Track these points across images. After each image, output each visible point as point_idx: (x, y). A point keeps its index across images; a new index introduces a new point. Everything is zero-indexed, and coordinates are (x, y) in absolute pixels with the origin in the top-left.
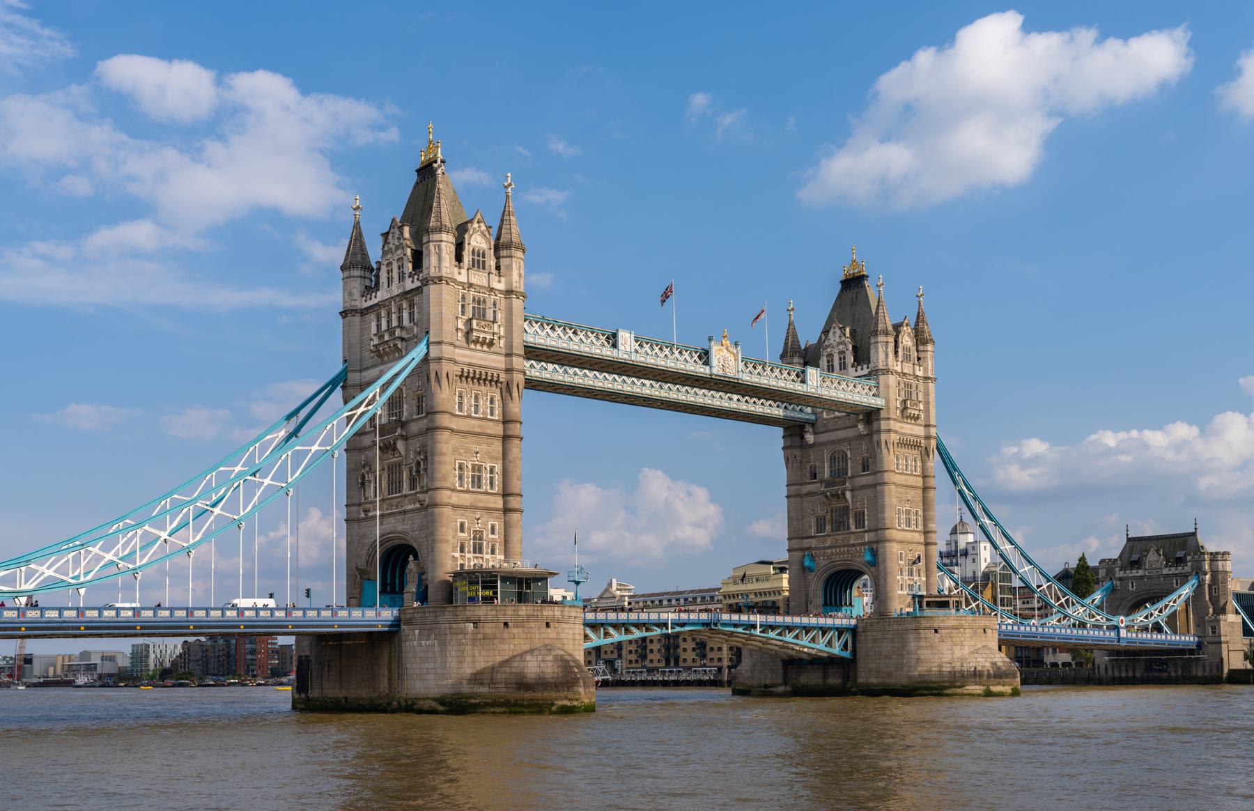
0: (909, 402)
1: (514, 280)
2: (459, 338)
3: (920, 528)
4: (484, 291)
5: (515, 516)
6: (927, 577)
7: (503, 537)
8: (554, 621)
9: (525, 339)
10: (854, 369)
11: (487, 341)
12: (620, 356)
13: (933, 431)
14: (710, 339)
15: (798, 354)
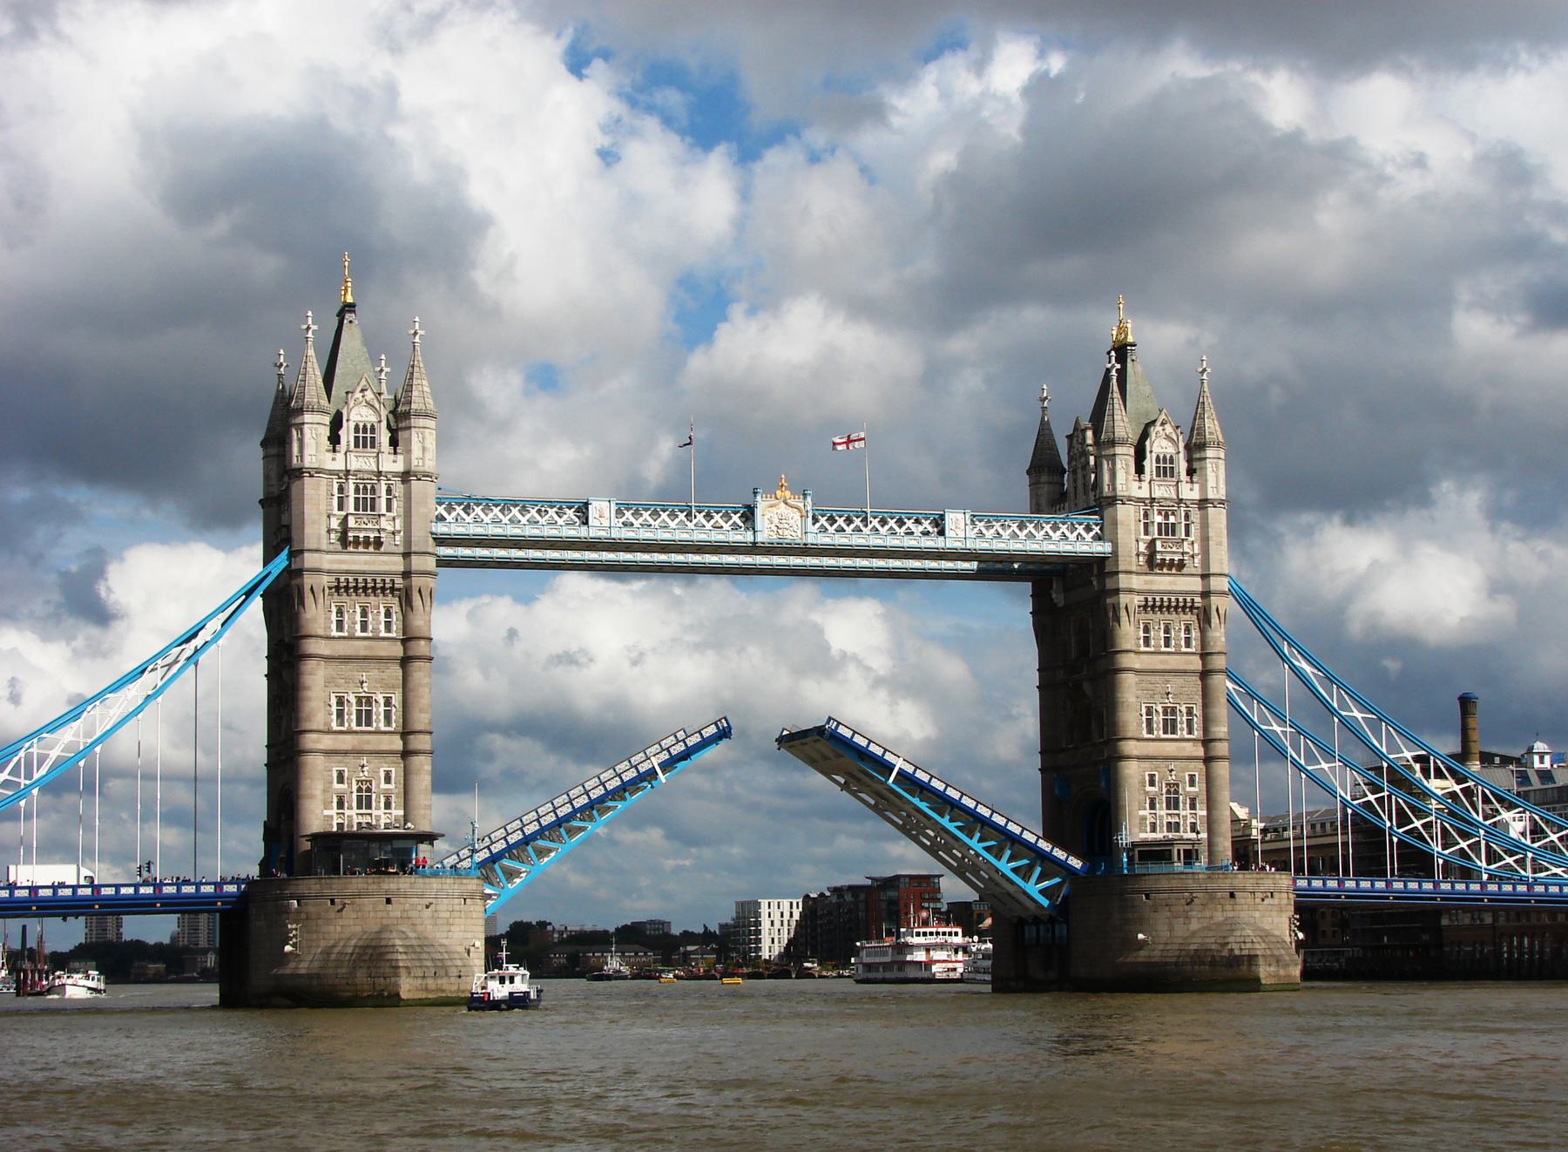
0: (1158, 544)
1: (413, 458)
2: (332, 541)
3: (1197, 734)
4: (369, 476)
5: (417, 761)
6: (1209, 809)
7: (402, 786)
8: (398, 894)
9: (434, 530)
10: (1094, 493)
11: (372, 540)
12: (591, 535)
13: (1218, 584)
14: (755, 493)
15: (1046, 469)
